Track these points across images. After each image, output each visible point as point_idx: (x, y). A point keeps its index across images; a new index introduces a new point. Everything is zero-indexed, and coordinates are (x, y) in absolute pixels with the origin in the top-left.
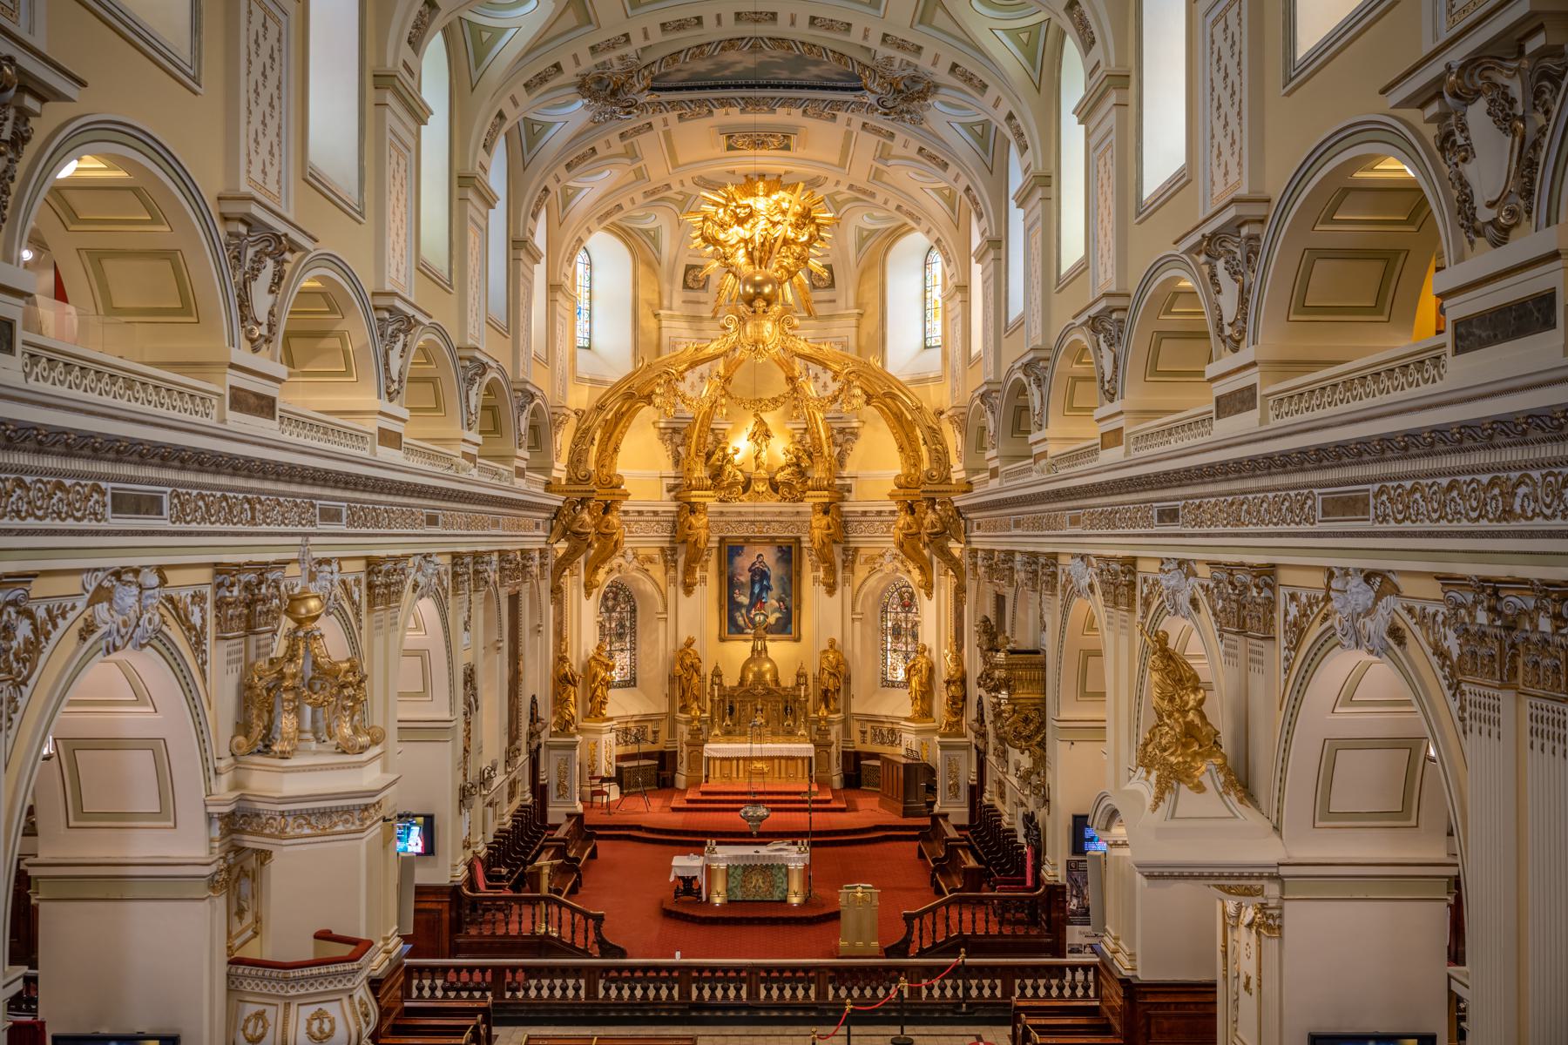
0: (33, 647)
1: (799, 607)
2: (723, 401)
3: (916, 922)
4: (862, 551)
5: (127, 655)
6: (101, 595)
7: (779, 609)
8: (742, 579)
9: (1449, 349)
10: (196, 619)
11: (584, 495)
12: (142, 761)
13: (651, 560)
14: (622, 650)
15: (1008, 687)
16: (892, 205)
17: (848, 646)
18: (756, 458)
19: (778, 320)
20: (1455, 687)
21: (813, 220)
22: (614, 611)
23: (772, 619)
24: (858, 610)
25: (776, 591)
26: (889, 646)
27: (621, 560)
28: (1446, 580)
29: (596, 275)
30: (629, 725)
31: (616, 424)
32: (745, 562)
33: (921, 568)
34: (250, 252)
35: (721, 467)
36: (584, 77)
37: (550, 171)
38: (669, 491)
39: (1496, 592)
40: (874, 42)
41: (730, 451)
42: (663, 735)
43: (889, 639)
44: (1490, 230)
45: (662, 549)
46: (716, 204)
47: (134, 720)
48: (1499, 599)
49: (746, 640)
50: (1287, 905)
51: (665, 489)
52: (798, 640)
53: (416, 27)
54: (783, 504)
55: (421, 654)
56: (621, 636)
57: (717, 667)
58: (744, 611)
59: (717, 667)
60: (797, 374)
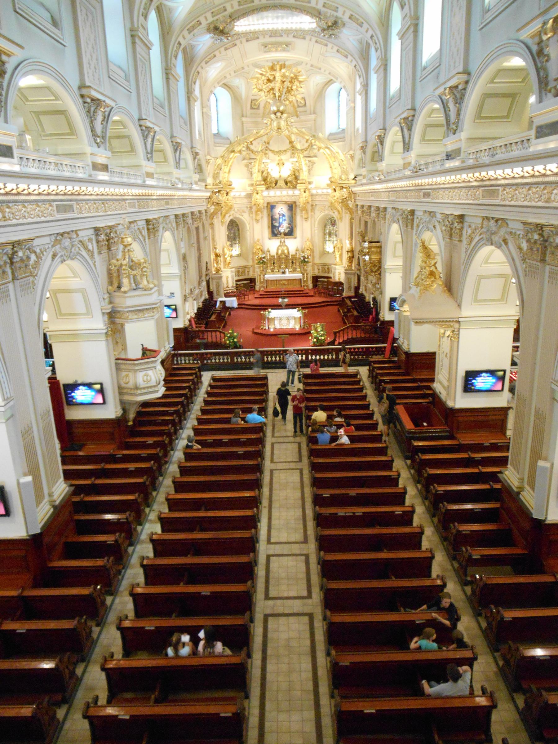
0: (37, 263)
1: (296, 226)
2: (267, 152)
3: (338, 334)
5: (69, 262)
6: (57, 242)
9: (533, 136)
10: (90, 247)
11: (220, 189)
12: (78, 297)
13: (244, 212)
15: (369, 255)
16: (327, 72)
19: (286, 120)
20: (524, 260)
24: (316, 226)
26: (327, 239)
28: (525, 223)
33: (338, 211)
34: (92, 109)
35: (267, 177)
36: (209, 25)
37: (199, 65)
39: (542, 228)
40: (320, 7)
41: (269, 171)
44: (553, 90)
45: (247, 207)
46: (262, 74)
47: (74, 283)
48: (543, 231)
49: (278, 239)
50: (461, 331)
52: (295, 238)
53: (145, 9)
55: (167, 250)
60: (293, 140)
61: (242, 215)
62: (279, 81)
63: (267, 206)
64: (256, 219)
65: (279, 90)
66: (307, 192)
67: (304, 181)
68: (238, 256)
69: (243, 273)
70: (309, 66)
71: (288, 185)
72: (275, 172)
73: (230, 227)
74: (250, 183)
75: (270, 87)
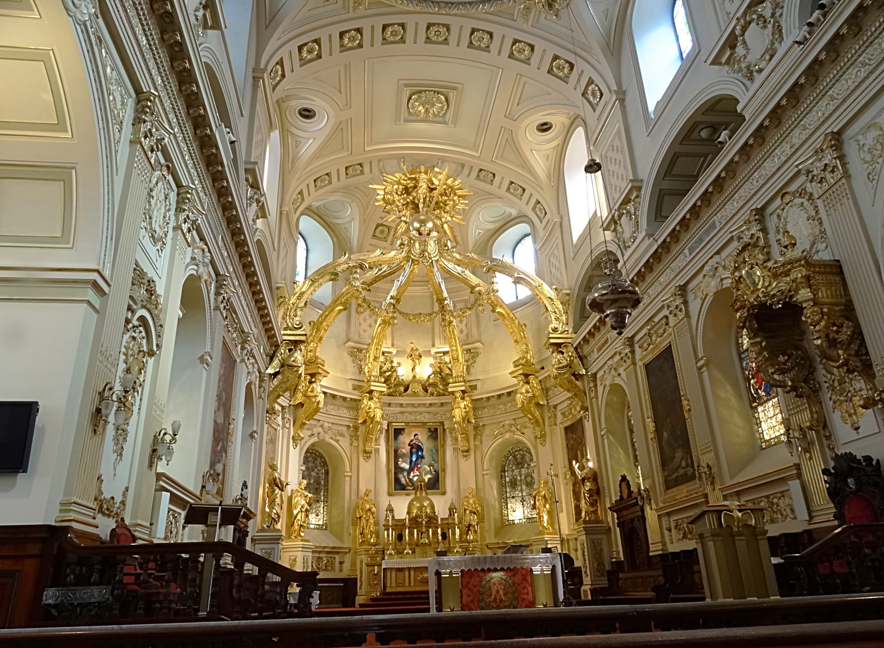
1: (444, 470)
2: (395, 315)
4: (487, 427)
7: (430, 472)
8: (404, 451)
11: (297, 338)
13: (342, 435)
14: (318, 501)
17: (482, 495)
18: (413, 370)
21: (455, 194)
22: (313, 471)
23: (427, 478)
24: (485, 468)
25: (427, 459)
26: (508, 495)
27: (320, 430)
29: (310, 255)
30: (321, 555)
31: (321, 323)
32: (405, 439)
38: (354, 389)
41: (395, 364)
42: (347, 566)
43: (508, 489)
45: (349, 427)
51: (350, 387)
52: (444, 493)
54: (432, 398)
56: (316, 491)
57: (390, 505)
58: (405, 474)
59: (390, 505)
61: (337, 441)
62: (425, 186)
63: (387, 430)
64: (365, 452)
65: (425, 199)
66: (467, 398)
67: (462, 379)
68: (319, 528)
69: (329, 566)
70: (474, 174)
71: (430, 390)
72: (404, 372)
73: (310, 465)
74: (356, 383)
75: (408, 200)
